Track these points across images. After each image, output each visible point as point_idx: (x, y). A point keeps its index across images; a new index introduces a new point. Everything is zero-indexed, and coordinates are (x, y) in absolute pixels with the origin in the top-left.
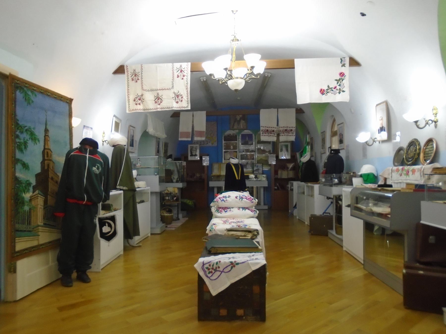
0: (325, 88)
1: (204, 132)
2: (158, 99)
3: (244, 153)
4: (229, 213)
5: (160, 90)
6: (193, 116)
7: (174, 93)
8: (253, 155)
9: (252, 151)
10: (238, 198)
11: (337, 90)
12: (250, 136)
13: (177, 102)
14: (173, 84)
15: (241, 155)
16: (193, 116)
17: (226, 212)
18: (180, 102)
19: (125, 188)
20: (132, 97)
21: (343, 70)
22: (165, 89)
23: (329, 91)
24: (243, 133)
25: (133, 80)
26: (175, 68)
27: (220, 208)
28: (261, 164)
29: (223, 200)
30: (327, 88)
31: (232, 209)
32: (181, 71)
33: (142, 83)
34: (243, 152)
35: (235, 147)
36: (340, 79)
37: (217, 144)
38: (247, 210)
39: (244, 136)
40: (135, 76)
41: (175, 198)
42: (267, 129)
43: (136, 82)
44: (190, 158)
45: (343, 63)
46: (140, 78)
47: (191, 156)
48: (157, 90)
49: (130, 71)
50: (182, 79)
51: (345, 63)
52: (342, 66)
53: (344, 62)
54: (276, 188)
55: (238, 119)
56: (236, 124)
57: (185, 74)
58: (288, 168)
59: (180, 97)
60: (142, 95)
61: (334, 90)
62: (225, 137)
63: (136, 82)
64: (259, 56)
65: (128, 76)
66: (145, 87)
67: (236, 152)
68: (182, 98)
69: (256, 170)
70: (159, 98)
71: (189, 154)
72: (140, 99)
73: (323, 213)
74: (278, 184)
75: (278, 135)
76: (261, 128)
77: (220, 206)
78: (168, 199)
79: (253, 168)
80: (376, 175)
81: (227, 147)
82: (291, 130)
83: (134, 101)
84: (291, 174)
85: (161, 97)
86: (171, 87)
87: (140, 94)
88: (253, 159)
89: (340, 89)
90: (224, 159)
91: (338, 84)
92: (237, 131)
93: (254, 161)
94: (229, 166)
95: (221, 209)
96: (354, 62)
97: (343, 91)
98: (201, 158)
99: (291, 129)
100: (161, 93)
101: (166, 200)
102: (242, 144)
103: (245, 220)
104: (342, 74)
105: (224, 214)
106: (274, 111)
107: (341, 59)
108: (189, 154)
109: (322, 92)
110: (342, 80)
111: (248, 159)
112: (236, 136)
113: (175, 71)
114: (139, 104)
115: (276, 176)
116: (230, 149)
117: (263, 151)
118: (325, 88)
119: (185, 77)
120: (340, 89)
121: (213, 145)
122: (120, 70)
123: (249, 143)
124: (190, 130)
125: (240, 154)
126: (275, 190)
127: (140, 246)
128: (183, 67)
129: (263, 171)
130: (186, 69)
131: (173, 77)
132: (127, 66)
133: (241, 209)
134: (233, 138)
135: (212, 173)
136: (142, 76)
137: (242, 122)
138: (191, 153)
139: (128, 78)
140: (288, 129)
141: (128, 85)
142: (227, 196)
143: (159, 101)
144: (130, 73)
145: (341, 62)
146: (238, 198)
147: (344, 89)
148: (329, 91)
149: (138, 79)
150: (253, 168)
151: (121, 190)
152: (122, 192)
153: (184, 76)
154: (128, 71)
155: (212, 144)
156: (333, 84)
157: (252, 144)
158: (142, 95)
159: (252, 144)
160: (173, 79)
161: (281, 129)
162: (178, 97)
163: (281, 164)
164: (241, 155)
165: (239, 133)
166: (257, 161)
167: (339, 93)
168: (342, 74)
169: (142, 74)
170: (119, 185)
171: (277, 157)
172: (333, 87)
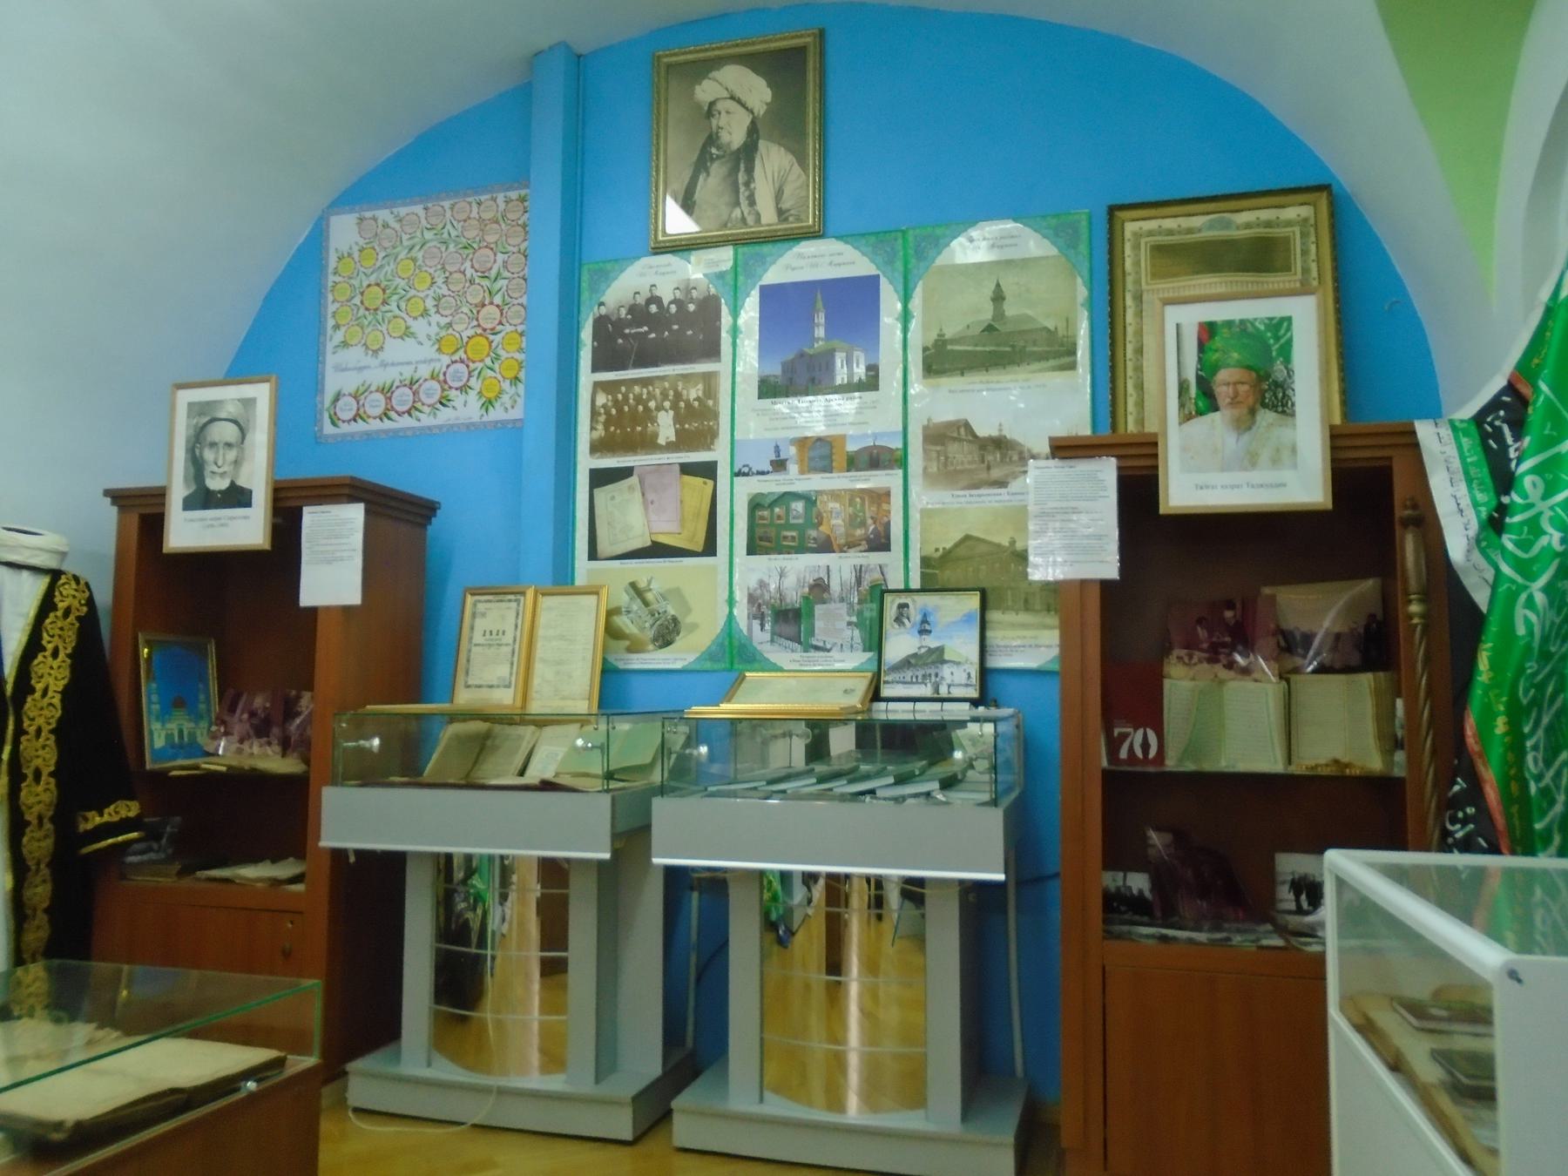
3: (773, 485)
8: (882, 496)
9: (875, 459)
12: (852, 303)
24: (775, 275)
28: (973, 601)
34: (779, 465)
35: (698, 425)
44: (187, 532)
47: (189, 504)
54: (1139, 882)
55: (734, 135)
56: (711, 185)
62: (600, 322)
67: (707, 471)
69: (906, 663)
71: (178, 492)
74: (1157, 839)
79: (875, 642)
81: (625, 430)
84: (1342, 726)
88: (880, 543)
90: (593, 555)
92: (724, 257)
93: (895, 568)
102: (768, 389)
108: (178, 492)
111: (826, 546)
112: (708, 310)
115: (1136, 739)
116: (648, 443)
117: (996, 455)
121: (496, 414)
123: (841, 376)
125: (747, 488)
129: (985, 673)
134: (686, 332)
137: (773, 160)
138: (197, 466)
150: (875, 642)
155: (488, 404)
157: (871, 382)
159: (871, 382)
164: (755, 505)
165: (734, 282)
166: (926, 562)
171: (1138, 491)
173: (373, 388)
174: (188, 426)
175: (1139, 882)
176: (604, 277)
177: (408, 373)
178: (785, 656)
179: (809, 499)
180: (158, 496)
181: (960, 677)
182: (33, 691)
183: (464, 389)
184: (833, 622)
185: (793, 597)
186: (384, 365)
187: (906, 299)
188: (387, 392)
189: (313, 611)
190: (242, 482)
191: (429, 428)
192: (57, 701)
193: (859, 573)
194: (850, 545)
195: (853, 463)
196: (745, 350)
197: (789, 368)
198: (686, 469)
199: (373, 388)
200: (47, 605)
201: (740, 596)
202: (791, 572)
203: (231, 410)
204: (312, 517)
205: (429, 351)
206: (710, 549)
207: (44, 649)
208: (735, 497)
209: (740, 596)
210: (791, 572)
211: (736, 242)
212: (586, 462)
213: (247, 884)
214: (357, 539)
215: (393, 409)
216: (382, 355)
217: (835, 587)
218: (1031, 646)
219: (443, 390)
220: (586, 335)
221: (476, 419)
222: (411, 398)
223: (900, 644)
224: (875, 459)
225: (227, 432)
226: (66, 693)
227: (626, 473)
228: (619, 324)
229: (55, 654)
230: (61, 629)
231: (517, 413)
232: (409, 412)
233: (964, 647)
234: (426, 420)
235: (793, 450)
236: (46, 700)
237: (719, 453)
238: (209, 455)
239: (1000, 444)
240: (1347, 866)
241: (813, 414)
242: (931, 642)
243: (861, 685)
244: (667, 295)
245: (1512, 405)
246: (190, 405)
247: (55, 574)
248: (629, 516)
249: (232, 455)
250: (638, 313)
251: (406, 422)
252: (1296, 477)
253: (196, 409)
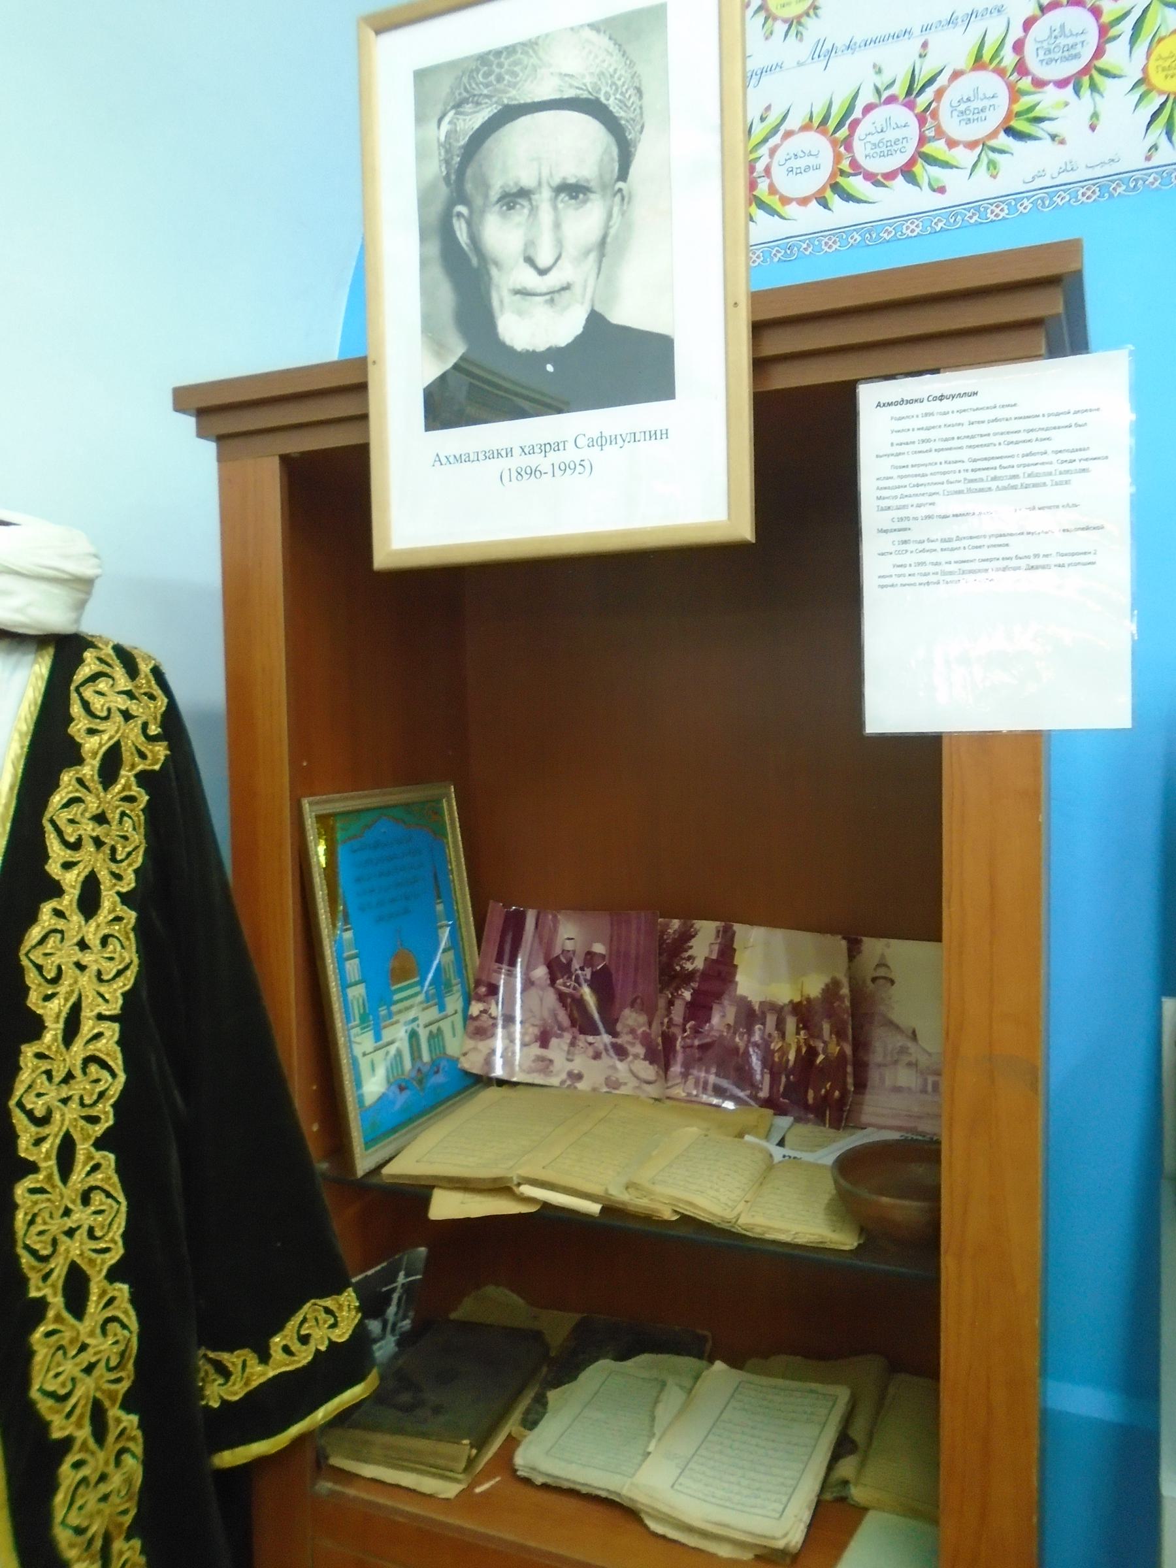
44: (442, 500)
47: (445, 407)
71: (404, 372)
98: (804, 452)
108: (404, 372)
138: (464, 275)
173: (793, 123)
174: (421, 155)
177: (898, 64)
180: (345, 389)
182: (34, 1027)
186: (824, 53)
188: (838, 127)
189: (922, 754)
190: (628, 313)
191: (975, 206)
192: (109, 1044)
199: (793, 123)
200: (49, 749)
204: (900, 427)
207: (57, 890)
215: (856, 167)
216: (814, 28)
219: (1015, 94)
221: (1133, 159)
222: (913, 131)
225: (563, 146)
226: (130, 1018)
229: (89, 902)
230: (100, 819)
232: (907, 172)
234: (964, 185)
236: (79, 1050)
238: (502, 236)
246: (421, 76)
247: (66, 649)
249: (584, 223)
251: (900, 199)
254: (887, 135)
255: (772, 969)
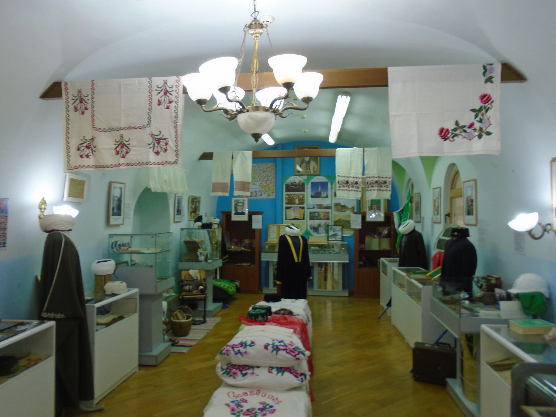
0: (450, 126)
1: (249, 183)
2: (122, 147)
3: (313, 210)
4: (248, 380)
5: (126, 128)
6: (232, 158)
7: (152, 135)
8: (328, 213)
9: (328, 207)
10: (270, 348)
11: (475, 130)
12: (324, 185)
13: (157, 153)
14: (149, 118)
15: (311, 213)
16: (232, 158)
17: (244, 375)
18: (162, 153)
19: (59, 316)
20: (74, 143)
21: (488, 89)
22: (135, 128)
23: (457, 132)
24: (312, 181)
25: (76, 109)
26: (154, 88)
27: (234, 366)
28: (340, 227)
29: (239, 352)
30: (454, 126)
31: (256, 371)
32: (166, 93)
33: (93, 116)
34: (314, 208)
35: (302, 201)
36: (481, 109)
37: (276, 196)
38: (287, 375)
39: (314, 185)
40: (81, 102)
41: (201, 287)
42: (346, 179)
43: (83, 113)
44: (235, 218)
45: (488, 75)
46: (89, 107)
47: (235, 214)
48: (120, 129)
49: (72, 92)
50: (168, 108)
51: (493, 75)
52: (486, 82)
53: (491, 72)
54: (362, 263)
57: (173, 98)
58: (380, 234)
59: (163, 144)
60: (93, 139)
61: (468, 130)
63: (83, 113)
64: (303, 60)
65: (67, 102)
66: (98, 124)
67: (303, 208)
68: (166, 144)
69: (332, 235)
70: (122, 145)
71: (233, 212)
72: (88, 147)
73: (437, 343)
75: (364, 191)
76: (338, 179)
77: (233, 363)
78: (189, 291)
79: (327, 232)
80: (547, 295)
81: (291, 201)
82: (385, 182)
83: (78, 149)
84: (385, 245)
85: (127, 143)
86: (146, 123)
87: (88, 137)
88: (328, 219)
89: (481, 129)
90: (286, 219)
91: (478, 119)
93: (330, 222)
94: (283, 239)
95: (234, 370)
96: (511, 74)
97: (488, 134)
99: (385, 180)
100: (127, 134)
101: (185, 291)
102: (312, 197)
103: (282, 396)
104: (486, 99)
105: (239, 380)
106: (357, 151)
107: (485, 68)
108: (233, 212)
109: (444, 134)
110: (487, 111)
111: (320, 219)
113: (154, 93)
114: (87, 156)
115: (362, 246)
116: (294, 203)
118: (450, 126)
119: (173, 104)
120: (481, 129)
121: (270, 197)
122: (54, 91)
123: (322, 196)
124: (228, 181)
126: (360, 266)
127: (101, 410)
128: (169, 84)
130: (174, 88)
131: (150, 104)
132: (66, 84)
133: (274, 371)
134: (300, 187)
135: (267, 240)
136: (93, 102)
138: (236, 209)
139: (68, 107)
140: (381, 179)
141: (68, 120)
142: (249, 343)
143: (124, 150)
144: (71, 97)
145: (484, 73)
146: (270, 348)
147: (489, 130)
148: (457, 132)
149: (86, 109)
150: (327, 232)
151: (50, 319)
152: (52, 323)
153: (170, 102)
154: (67, 93)
155: (268, 196)
156: (468, 118)
158: (93, 139)
159: (327, 197)
160: (150, 109)
161: (369, 180)
162: (158, 143)
163: (369, 228)
164: (311, 213)
166: (334, 222)
167: (480, 136)
168: (486, 99)
169: (93, 98)
170: (47, 311)
171: (364, 218)
172: (467, 124)
175: (362, 263)
176: (287, 178)
177: (255, 190)
178: (315, 234)
179: (318, 213)
181: (339, 237)
183: (264, 193)
184: (321, 230)
185: (316, 226)
187: (332, 185)
189: (254, 229)
193: (325, 223)
194: (324, 219)
195: (325, 208)
196: (308, 191)
197: (315, 194)
198: (301, 208)
201: (308, 226)
202: (316, 223)
203: (241, 201)
204: (254, 217)
205: (258, 187)
206: (304, 219)
208: (307, 212)
209: (308, 226)
210: (316, 223)
211: (308, 175)
212: (285, 206)
213: (244, 266)
214: (261, 220)
217: (322, 225)
218: (348, 233)
220: (284, 187)
223: (331, 233)
224: (328, 207)
225: (241, 204)
227: (291, 207)
228: (289, 186)
231: (274, 197)
233: (339, 233)
234: (258, 198)
235: (315, 206)
237: (305, 205)
239: (344, 207)
240: (383, 260)
241: (318, 201)
242: (335, 233)
243: (326, 238)
244: (297, 182)
245: (402, 211)
248: (292, 214)
250: (292, 184)
251: (255, 198)
252: (381, 218)
253: (235, 201)
254: (254, 194)
255: (247, 241)
